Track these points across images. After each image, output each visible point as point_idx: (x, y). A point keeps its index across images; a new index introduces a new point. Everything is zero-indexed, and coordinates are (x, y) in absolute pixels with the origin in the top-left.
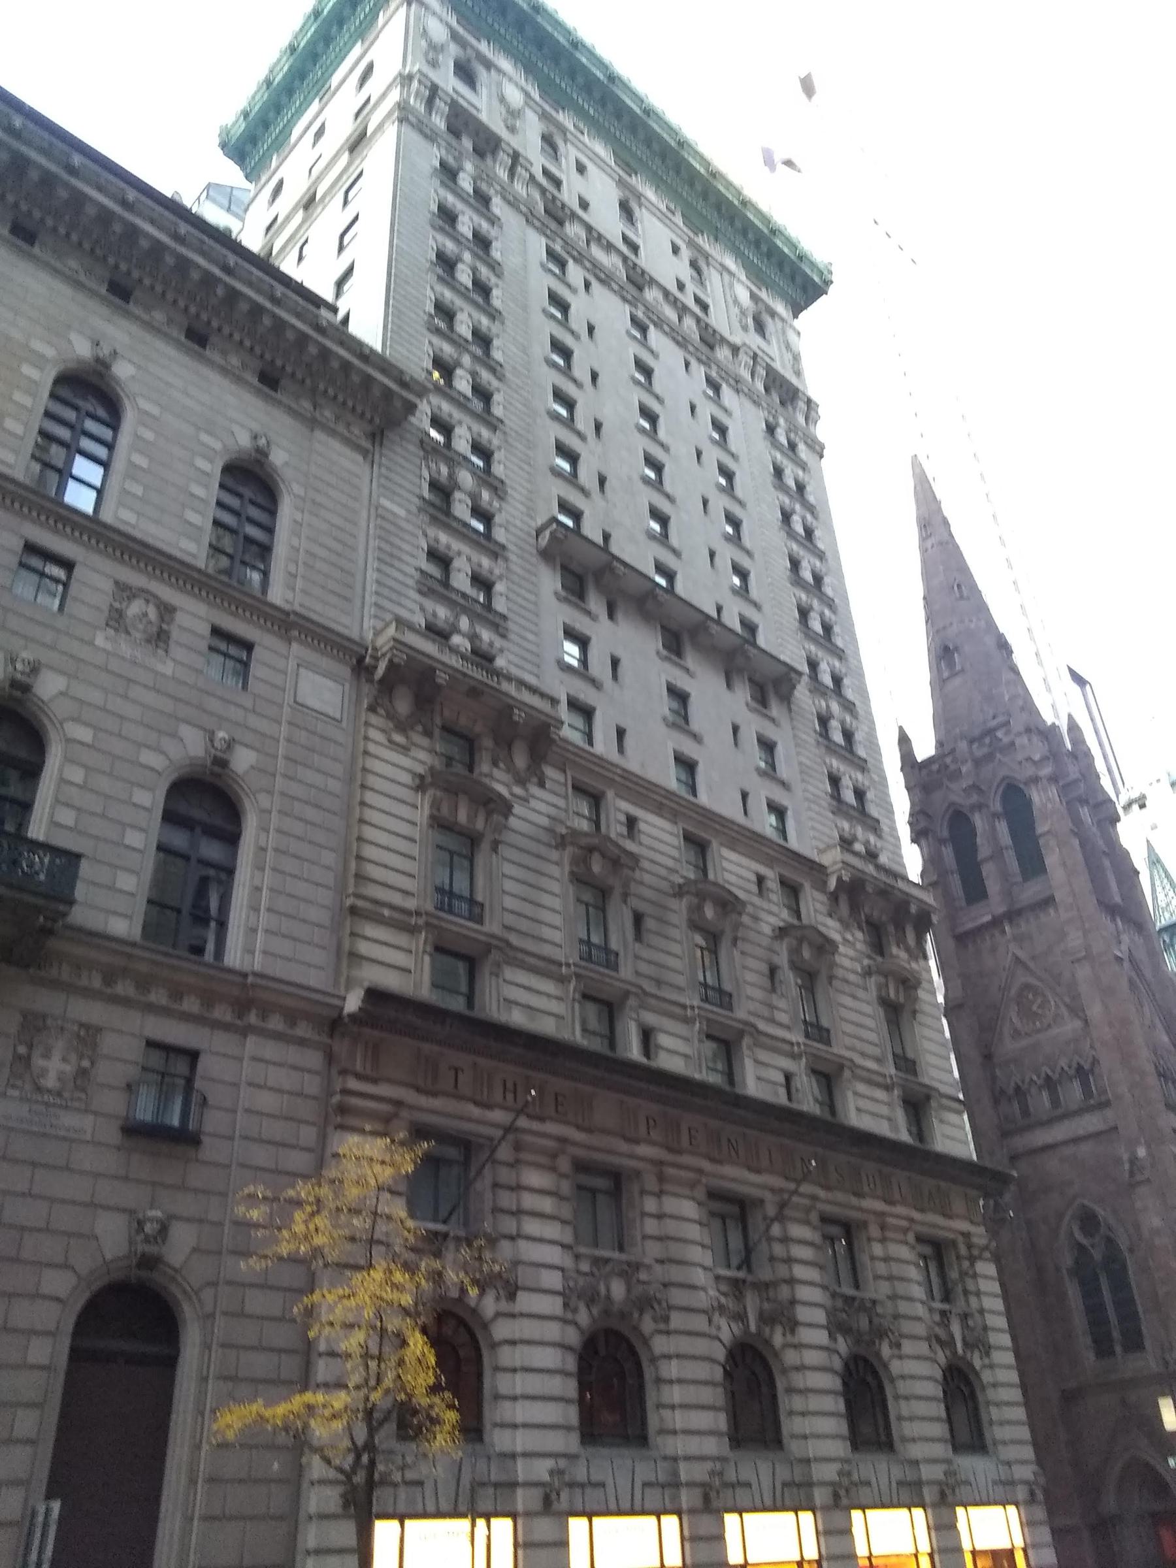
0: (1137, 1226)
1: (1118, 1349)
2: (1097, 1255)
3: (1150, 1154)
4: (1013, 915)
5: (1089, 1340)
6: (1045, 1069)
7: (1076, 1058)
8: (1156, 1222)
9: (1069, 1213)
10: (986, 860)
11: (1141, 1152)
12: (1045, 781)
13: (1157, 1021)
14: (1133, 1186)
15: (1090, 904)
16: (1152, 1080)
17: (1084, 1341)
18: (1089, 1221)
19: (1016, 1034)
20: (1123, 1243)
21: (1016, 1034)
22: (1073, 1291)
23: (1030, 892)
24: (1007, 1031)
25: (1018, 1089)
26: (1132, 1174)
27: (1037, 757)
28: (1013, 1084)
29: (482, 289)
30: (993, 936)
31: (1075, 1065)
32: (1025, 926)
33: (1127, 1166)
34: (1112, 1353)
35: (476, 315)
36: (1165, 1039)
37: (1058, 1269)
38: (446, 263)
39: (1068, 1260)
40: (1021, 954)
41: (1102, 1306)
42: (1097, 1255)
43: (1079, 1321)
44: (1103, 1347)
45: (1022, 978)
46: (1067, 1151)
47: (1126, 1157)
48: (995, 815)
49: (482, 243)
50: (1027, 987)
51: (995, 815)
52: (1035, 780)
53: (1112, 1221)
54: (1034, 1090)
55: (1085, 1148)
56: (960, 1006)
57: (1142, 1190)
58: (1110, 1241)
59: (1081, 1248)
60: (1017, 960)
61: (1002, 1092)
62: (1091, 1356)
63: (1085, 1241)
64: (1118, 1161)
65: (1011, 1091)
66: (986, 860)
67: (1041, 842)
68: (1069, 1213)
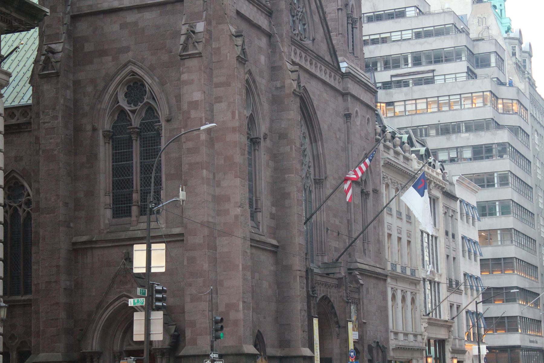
0: (179, 98)
1: (135, 210)
2: (136, 122)
3: (208, 31)
5: (109, 200)
8: (197, 96)
9: (118, 79)
11: (200, 27)
14: (183, 58)
17: (104, 200)
18: (135, 88)
20: (163, 113)
22: (104, 152)
26: (185, 47)
33: (183, 38)
34: (128, 213)
37: (94, 129)
39: (106, 124)
41: (129, 170)
42: (136, 122)
43: (104, 180)
44: (121, 207)
46: (131, 17)
47: (184, 29)
53: (156, 89)
55: (149, 16)
57: (193, 63)
58: (151, 110)
59: (122, 111)
62: (109, 213)
63: (127, 108)
64: (177, 34)
68: (118, 79)
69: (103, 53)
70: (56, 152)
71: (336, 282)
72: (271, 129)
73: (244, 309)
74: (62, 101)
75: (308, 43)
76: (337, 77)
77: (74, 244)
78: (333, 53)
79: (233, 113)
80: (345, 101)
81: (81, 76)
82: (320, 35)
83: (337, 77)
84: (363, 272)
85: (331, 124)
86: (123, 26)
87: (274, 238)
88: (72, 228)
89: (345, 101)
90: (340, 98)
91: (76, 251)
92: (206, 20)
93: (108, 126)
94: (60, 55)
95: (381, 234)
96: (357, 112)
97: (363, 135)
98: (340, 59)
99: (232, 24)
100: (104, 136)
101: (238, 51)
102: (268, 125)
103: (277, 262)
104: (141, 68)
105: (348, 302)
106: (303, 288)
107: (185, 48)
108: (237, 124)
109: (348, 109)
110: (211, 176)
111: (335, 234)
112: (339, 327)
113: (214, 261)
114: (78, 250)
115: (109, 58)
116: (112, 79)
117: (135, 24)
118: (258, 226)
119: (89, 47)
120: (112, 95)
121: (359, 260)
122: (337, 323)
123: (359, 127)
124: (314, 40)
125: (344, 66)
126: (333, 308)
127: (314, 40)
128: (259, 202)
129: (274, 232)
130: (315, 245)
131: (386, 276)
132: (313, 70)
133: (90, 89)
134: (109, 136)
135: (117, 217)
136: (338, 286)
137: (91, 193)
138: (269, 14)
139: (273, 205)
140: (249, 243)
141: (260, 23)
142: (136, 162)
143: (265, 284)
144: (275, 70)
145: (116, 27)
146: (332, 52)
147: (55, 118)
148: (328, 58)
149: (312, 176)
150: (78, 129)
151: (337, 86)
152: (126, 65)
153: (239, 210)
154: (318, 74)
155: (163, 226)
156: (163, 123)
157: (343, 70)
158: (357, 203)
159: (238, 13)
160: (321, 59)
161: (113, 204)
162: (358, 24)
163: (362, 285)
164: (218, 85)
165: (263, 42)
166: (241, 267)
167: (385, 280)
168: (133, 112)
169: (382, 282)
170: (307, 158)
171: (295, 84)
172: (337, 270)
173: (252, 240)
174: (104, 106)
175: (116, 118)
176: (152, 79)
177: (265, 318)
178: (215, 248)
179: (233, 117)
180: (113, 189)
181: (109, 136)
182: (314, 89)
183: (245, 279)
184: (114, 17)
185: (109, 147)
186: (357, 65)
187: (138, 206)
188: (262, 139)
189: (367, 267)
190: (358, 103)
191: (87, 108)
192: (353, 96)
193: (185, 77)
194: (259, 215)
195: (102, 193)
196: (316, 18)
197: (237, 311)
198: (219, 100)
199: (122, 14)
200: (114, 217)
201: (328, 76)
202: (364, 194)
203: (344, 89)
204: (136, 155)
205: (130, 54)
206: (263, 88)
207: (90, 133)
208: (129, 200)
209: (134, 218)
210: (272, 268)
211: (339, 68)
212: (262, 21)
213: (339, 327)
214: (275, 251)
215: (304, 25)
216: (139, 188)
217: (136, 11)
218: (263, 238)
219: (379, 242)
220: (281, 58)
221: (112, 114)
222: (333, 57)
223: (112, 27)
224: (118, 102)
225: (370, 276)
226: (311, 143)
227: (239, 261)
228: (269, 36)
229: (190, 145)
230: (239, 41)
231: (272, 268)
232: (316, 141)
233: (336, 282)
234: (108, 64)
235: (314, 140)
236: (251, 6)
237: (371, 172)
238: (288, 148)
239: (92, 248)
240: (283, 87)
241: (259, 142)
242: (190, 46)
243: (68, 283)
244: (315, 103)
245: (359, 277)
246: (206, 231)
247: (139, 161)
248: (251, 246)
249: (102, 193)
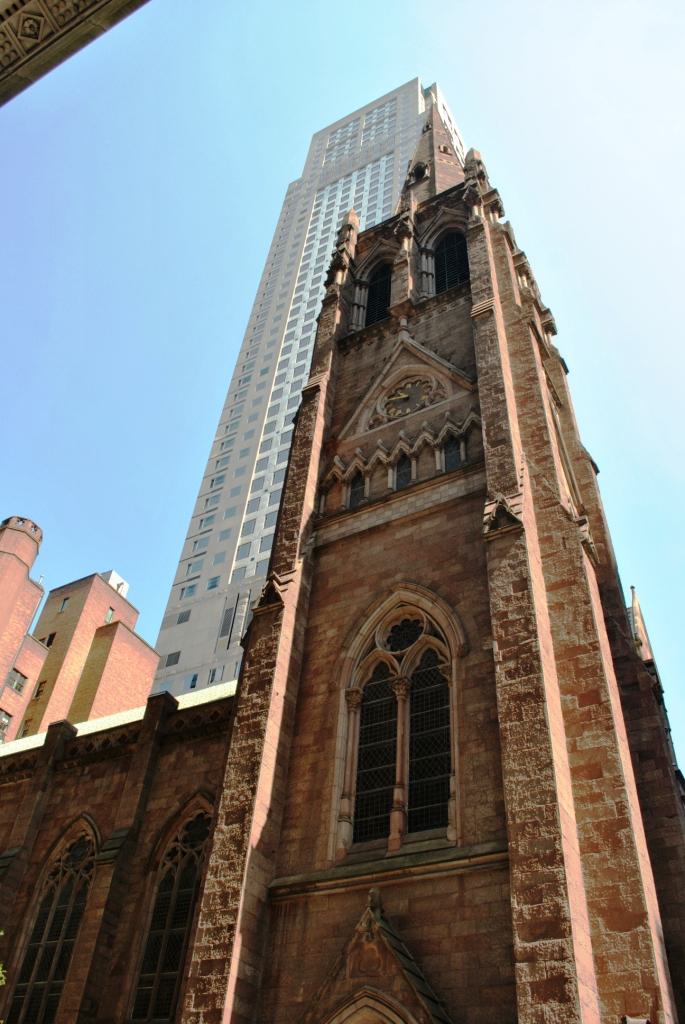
5: (348, 806)
34: (384, 829)
62: (346, 830)
119: (333, 582)
135: (360, 841)
142: (403, 736)
161: (356, 816)
180: (357, 790)
187: (404, 812)
195: (336, 793)
200: (355, 841)
204: (404, 724)
208: (388, 804)
216: (406, 781)
247: (407, 737)
249: (336, 793)
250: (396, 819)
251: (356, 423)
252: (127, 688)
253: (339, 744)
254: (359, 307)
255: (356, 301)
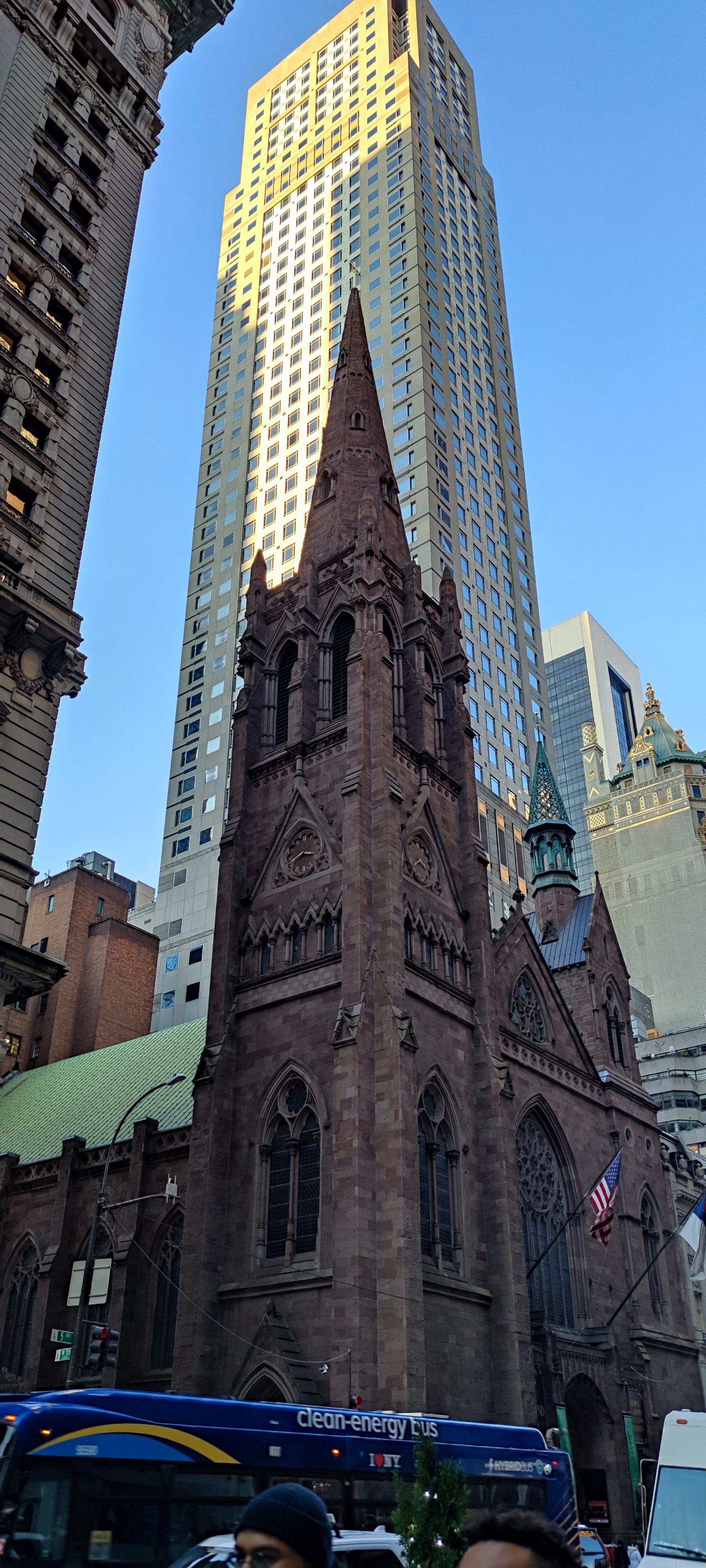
2: (295, 1133)
4: (305, 750)
5: (261, 1234)
6: (295, 916)
7: (327, 904)
8: (351, 1092)
10: (294, 688)
11: (357, 1010)
12: (372, 607)
13: (445, 887)
14: (337, 1047)
15: (382, 741)
16: (396, 933)
17: (257, 1233)
18: (296, 1090)
19: (280, 879)
21: (280, 879)
22: (260, 1172)
23: (337, 726)
24: (272, 872)
25: (264, 939)
26: (339, 1035)
27: (370, 583)
28: (260, 933)
29: (81, 215)
30: (285, 773)
31: (323, 912)
32: (316, 762)
35: (68, 236)
36: (450, 905)
37: (251, 1145)
38: (44, 181)
40: (304, 791)
42: (295, 1133)
43: (258, 1210)
45: (300, 818)
46: (293, 1009)
48: (322, 646)
49: (89, 170)
50: (303, 828)
51: (322, 646)
52: (362, 603)
53: (316, 1090)
54: (280, 941)
55: (311, 1005)
56: (230, 843)
57: (347, 1052)
59: (282, 1122)
60: (299, 798)
61: (249, 942)
62: (261, 1251)
63: (286, 1116)
65: (256, 941)
66: (294, 688)
67: (349, 668)
69: (263, 1053)
70: (203, 1175)
71: (603, 1355)
72: (476, 1141)
73: (410, 1385)
74: (215, 1112)
75: (546, 1045)
76: (596, 1088)
77: (221, 1294)
78: (587, 1059)
79: (396, 1113)
80: (609, 1117)
81: (243, 1081)
82: (564, 1036)
83: (596, 1088)
84: (651, 1344)
85: (589, 1145)
86: (285, 1020)
87: (485, 1287)
88: (220, 1272)
89: (609, 1117)
90: (602, 1114)
91: (222, 1303)
92: (364, 1001)
93: (266, 1141)
94: (217, 1058)
95: (683, 1291)
96: (628, 1131)
97: (641, 1160)
98: (598, 1068)
99: (398, 1006)
100: (261, 1152)
101: (402, 1035)
102: (471, 1135)
103: (489, 1321)
104: (301, 1066)
105: (621, 1386)
106: (527, 1359)
107: (339, 1035)
108: (400, 1126)
109: (613, 1127)
110: (369, 1196)
111: (605, 1289)
112: (612, 1422)
113: (370, 1314)
114: (224, 1302)
115: (270, 1059)
116: (271, 1083)
117: (298, 1015)
118: (458, 1268)
119: (252, 1047)
120: (271, 1102)
121: (645, 1326)
122: (608, 1416)
123: (633, 1150)
124: (553, 1041)
125: (604, 1076)
126: (599, 1393)
127: (553, 1041)
128: (459, 1236)
129: (483, 1279)
130: (574, 1304)
131: (697, 1351)
132: (555, 1076)
133: (249, 1096)
134: (267, 1152)
136: (605, 1362)
137: (243, 1226)
138: (470, 1002)
139: (481, 1240)
140: (420, 1287)
141: (456, 1013)
143: (469, 1352)
144: (478, 1067)
145: (279, 1021)
146: (585, 1058)
147: (206, 1132)
148: (578, 1064)
149: (565, 1211)
150: (235, 1146)
151: (595, 1097)
152: (286, 1065)
153: (402, 1240)
154: (564, 1081)
155: (317, 1266)
156: (322, 1131)
157: (604, 1080)
158: (636, 1246)
159: (409, 993)
160: (569, 1066)
162: (626, 1030)
163: (647, 1362)
164: (380, 1079)
165: (463, 1034)
166: (405, 1322)
167: (696, 1358)
168: (292, 1120)
169: (690, 1360)
170: (555, 1185)
171: (502, 1084)
172: (602, 1339)
173: (425, 1283)
174: (262, 1116)
175: (276, 1130)
176: (312, 1078)
177: (468, 1402)
178: (374, 1294)
179: (396, 1118)
181: (267, 1152)
182: (556, 1099)
183: (412, 1340)
184: (277, 1011)
185: (267, 1166)
186: (629, 1077)
188: (461, 1153)
189: (661, 1338)
190: (630, 1120)
191: (245, 1120)
192: (619, 1111)
193: (338, 1070)
194: (459, 1254)
195: (254, 1225)
196: (557, 1017)
197: (401, 1388)
198: (380, 1097)
199: (285, 1006)
201: (580, 1085)
202: (649, 1236)
203: (606, 1102)
205: (291, 1050)
206: (462, 1089)
207: (246, 1150)
209: (287, 1257)
210: (482, 1329)
211: (599, 1078)
212: (461, 1011)
213: (612, 1422)
214: (486, 1304)
215: (540, 1024)
216: (296, 1217)
217: (299, 1001)
218: (463, 1286)
219: (680, 1303)
220: (486, 1052)
221: (271, 1125)
222: (587, 1063)
223: (274, 1021)
224: (277, 1109)
225: (668, 1351)
226: (560, 1166)
227: (403, 1314)
228: (471, 1028)
229: (341, 1155)
230: (405, 1024)
231: (482, 1329)
232: (565, 1165)
233: (603, 1355)
234: (269, 1066)
235: (562, 1163)
236: (441, 992)
237: (658, 1208)
238: (498, 1165)
239: (241, 1299)
240: (489, 1088)
241: (457, 1157)
242: (344, 1031)
243: (208, 1348)
244: (560, 1116)
245: (643, 1350)
246: (357, 1271)
248: (424, 1291)
249: (254, 1225)
250: (288, 1245)
251: (264, 878)
252: (131, 985)
253: (256, 1188)
254: (269, 708)
255: (266, 702)
